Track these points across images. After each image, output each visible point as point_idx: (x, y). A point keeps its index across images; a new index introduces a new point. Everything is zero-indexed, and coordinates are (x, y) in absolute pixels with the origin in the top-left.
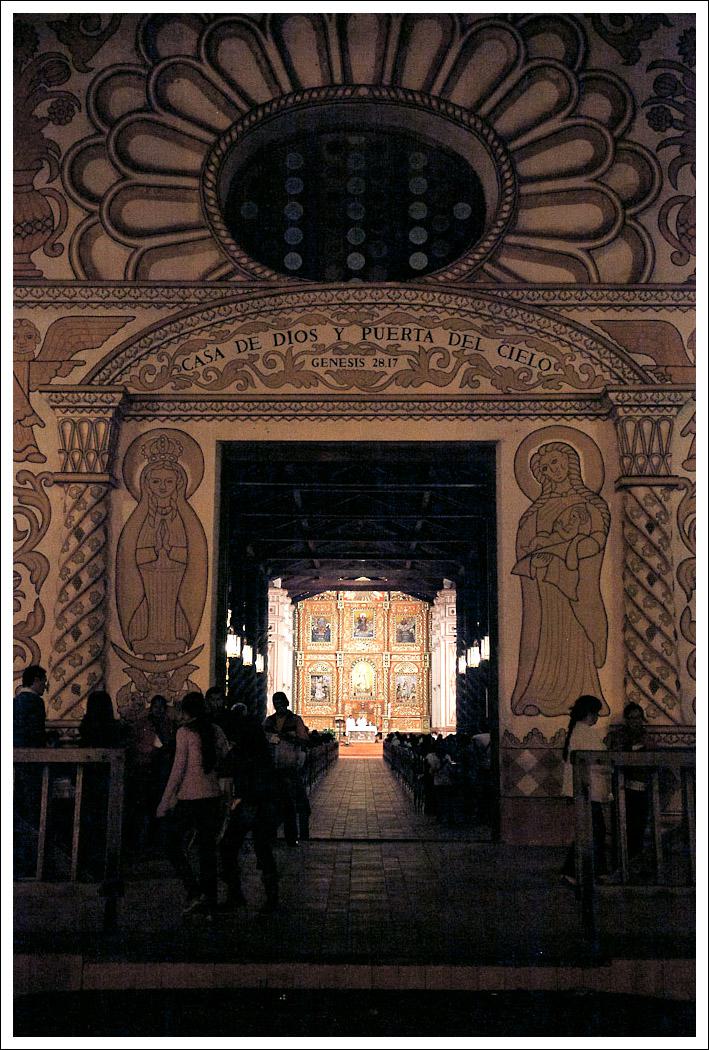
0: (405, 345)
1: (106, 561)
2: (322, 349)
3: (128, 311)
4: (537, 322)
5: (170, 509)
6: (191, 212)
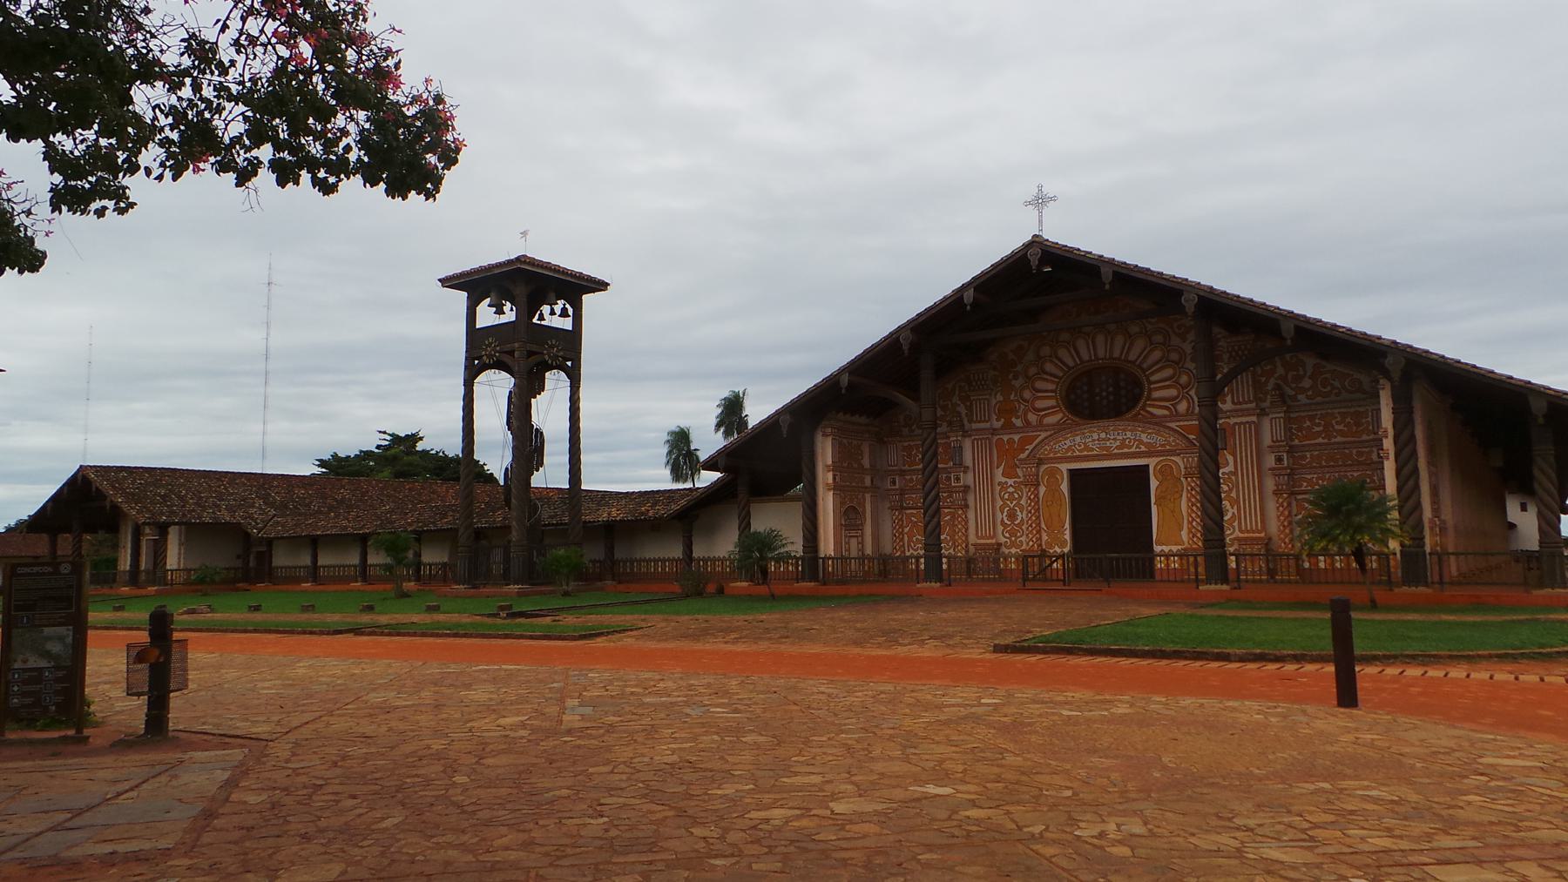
0: (1118, 437)
1: (1038, 505)
2: (1094, 440)
3: (1039, 433)
4: (1157, 428)
5: (1053, 489)
6: (1052, 402)
